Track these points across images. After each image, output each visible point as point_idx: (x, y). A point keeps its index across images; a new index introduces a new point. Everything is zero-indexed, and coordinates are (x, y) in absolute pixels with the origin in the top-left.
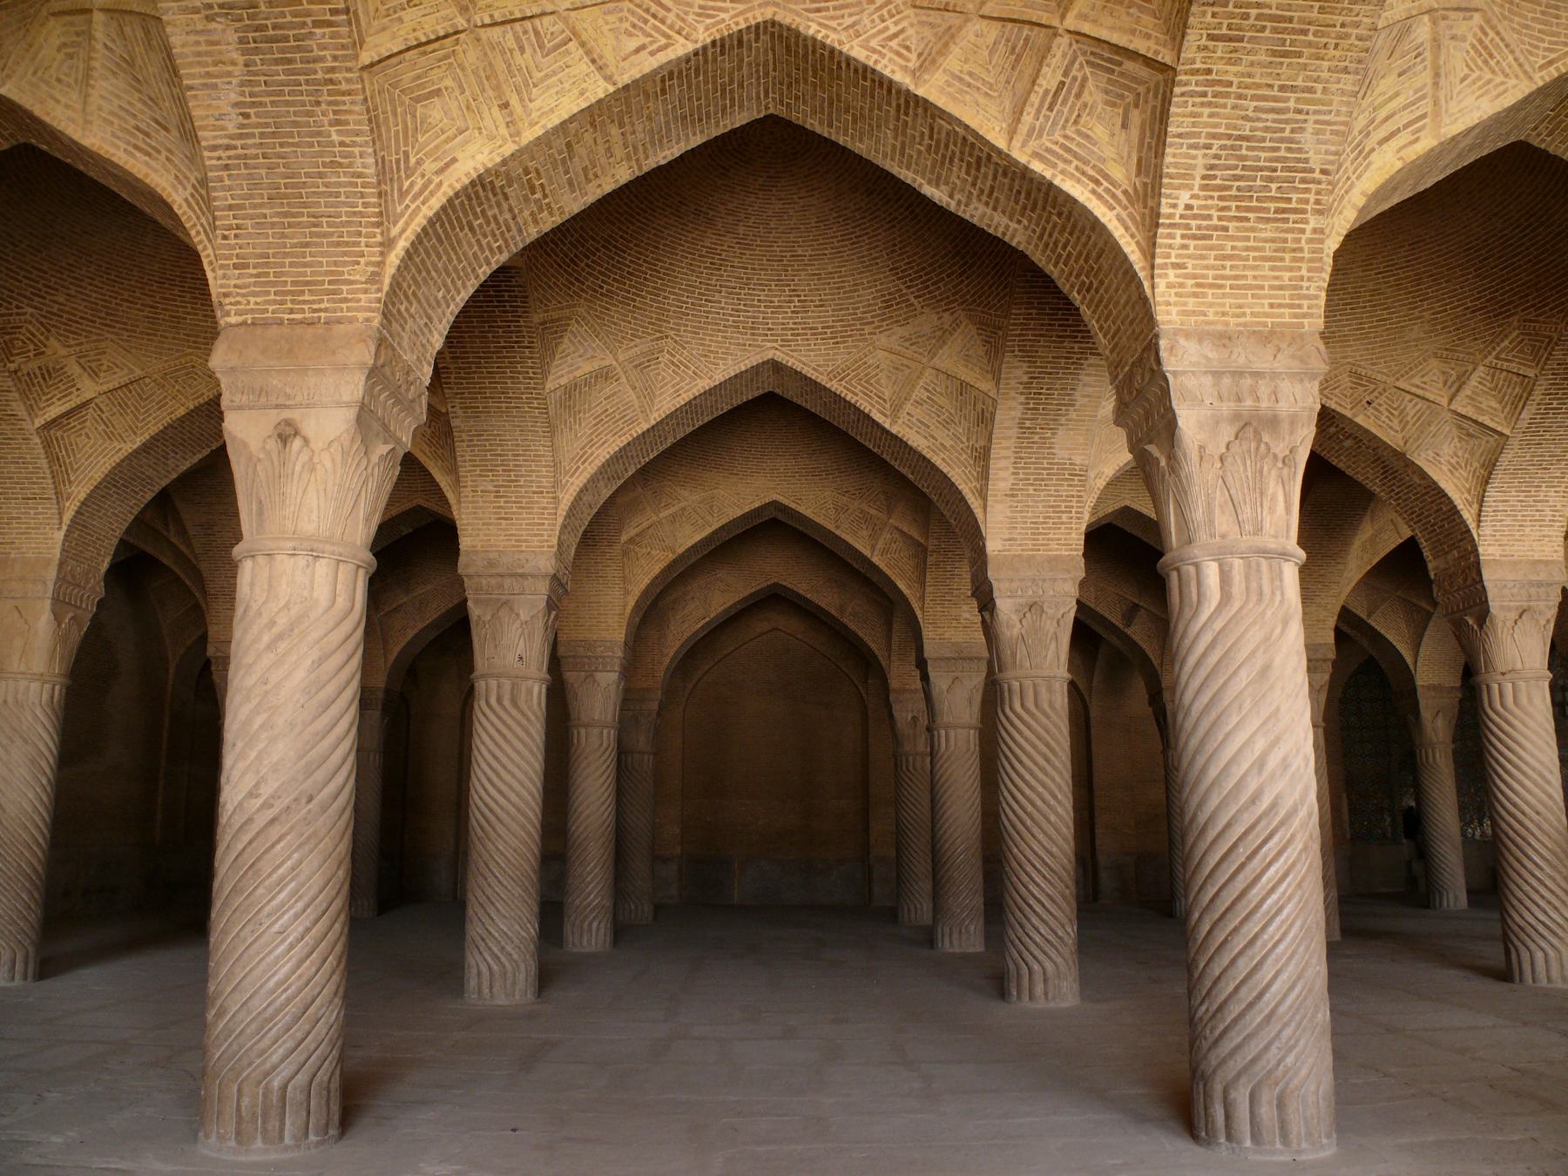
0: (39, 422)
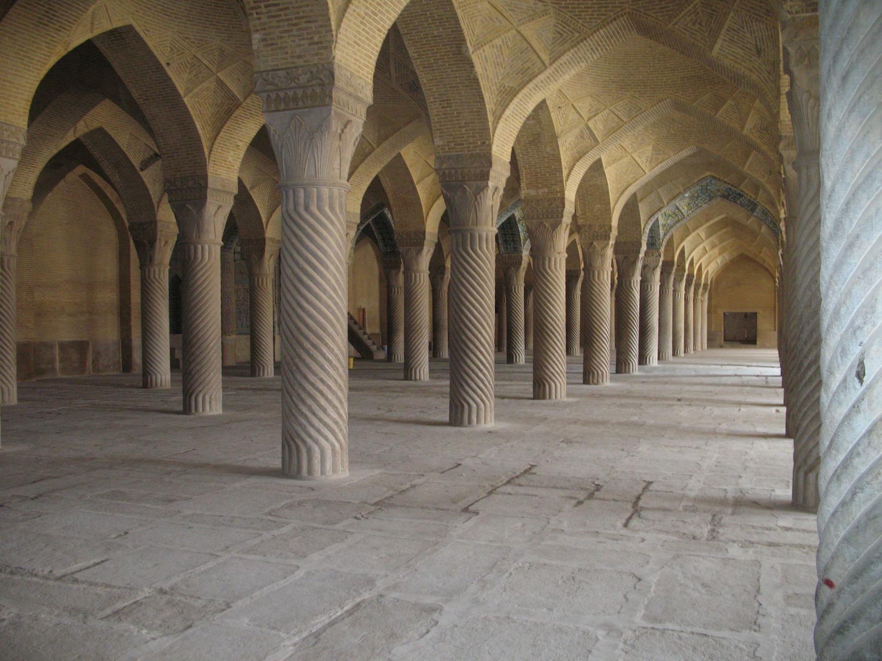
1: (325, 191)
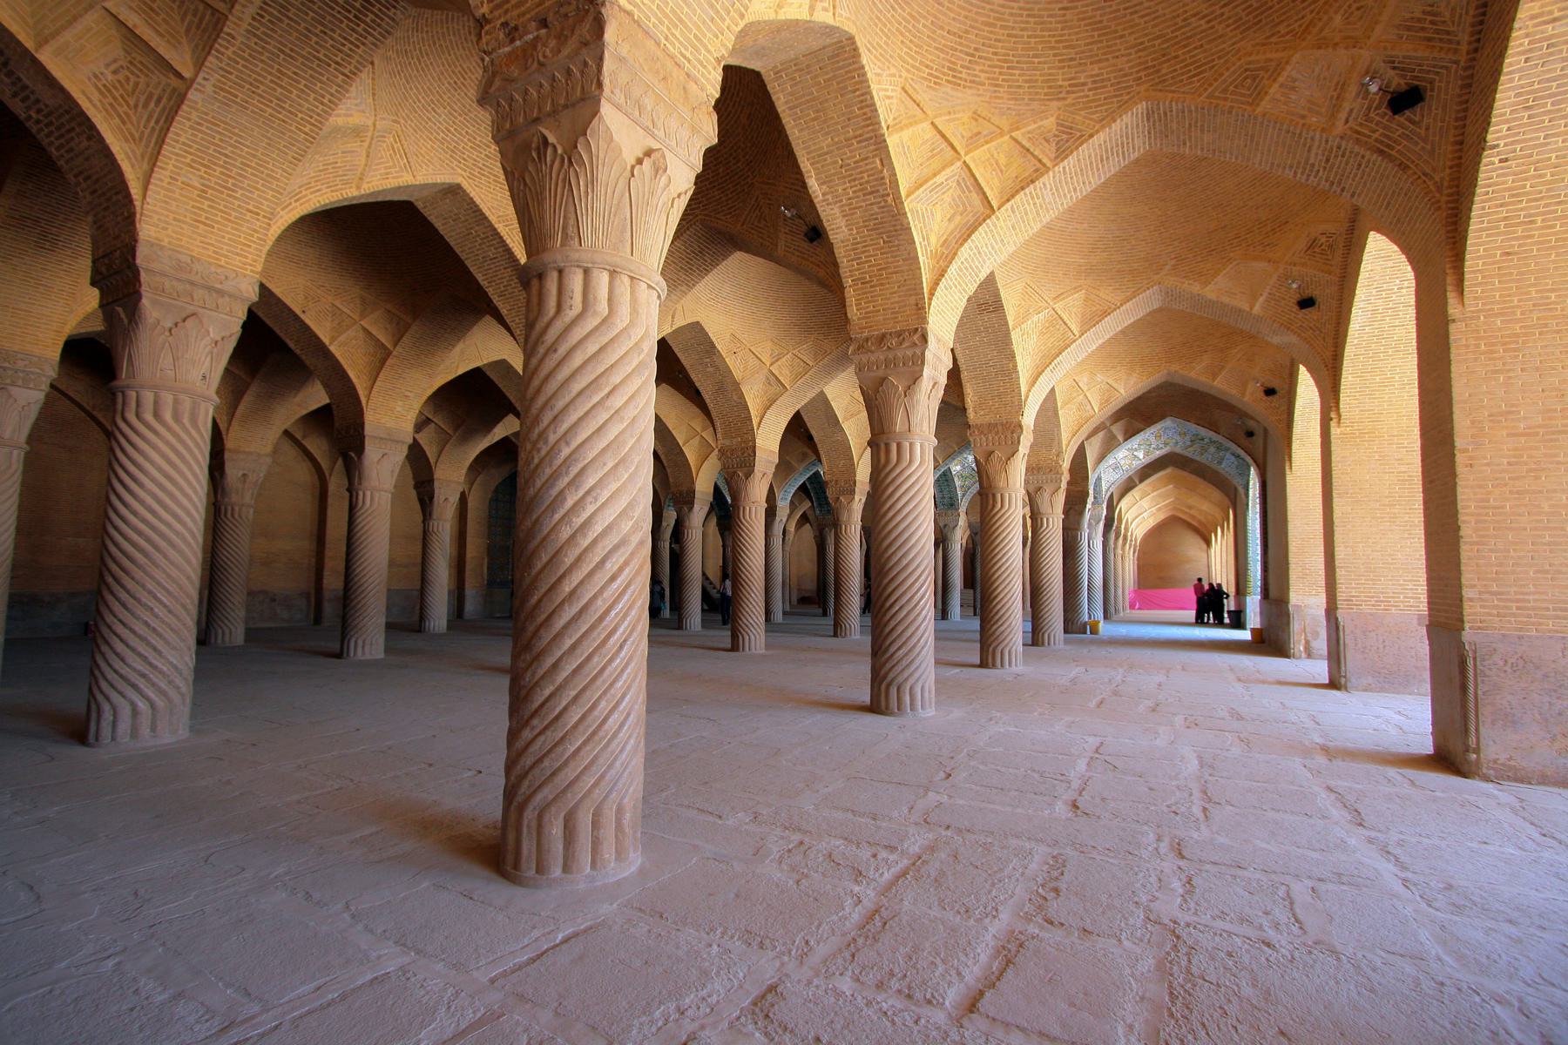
1: (148, 397)
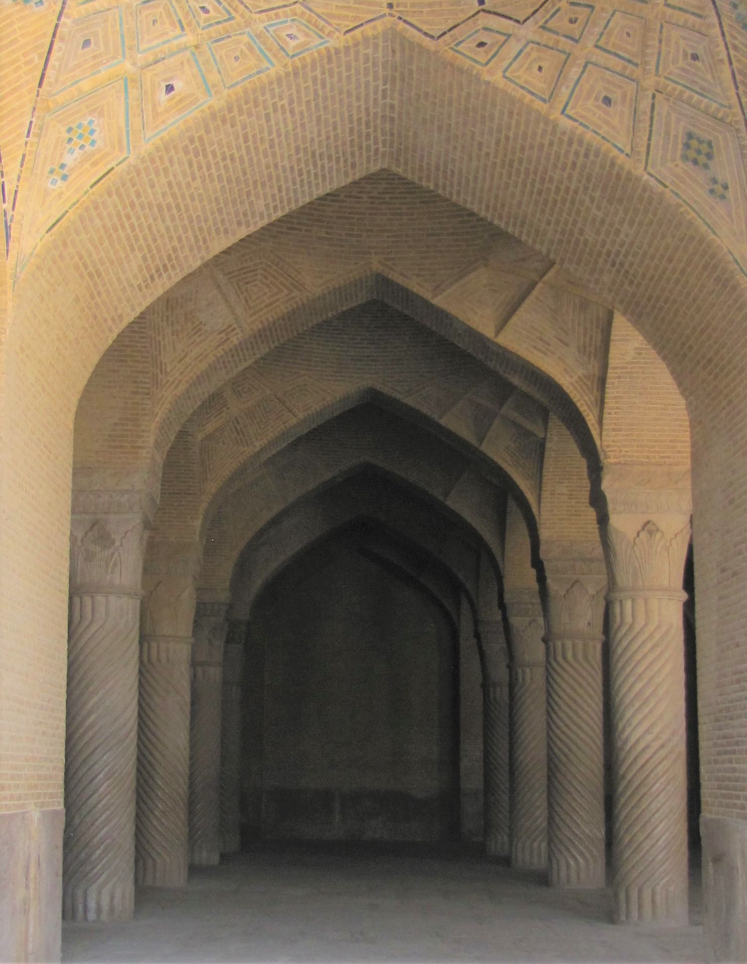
0: (200, 437)
1: (559, 644)
